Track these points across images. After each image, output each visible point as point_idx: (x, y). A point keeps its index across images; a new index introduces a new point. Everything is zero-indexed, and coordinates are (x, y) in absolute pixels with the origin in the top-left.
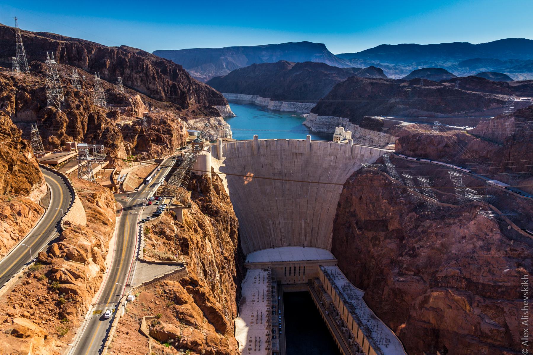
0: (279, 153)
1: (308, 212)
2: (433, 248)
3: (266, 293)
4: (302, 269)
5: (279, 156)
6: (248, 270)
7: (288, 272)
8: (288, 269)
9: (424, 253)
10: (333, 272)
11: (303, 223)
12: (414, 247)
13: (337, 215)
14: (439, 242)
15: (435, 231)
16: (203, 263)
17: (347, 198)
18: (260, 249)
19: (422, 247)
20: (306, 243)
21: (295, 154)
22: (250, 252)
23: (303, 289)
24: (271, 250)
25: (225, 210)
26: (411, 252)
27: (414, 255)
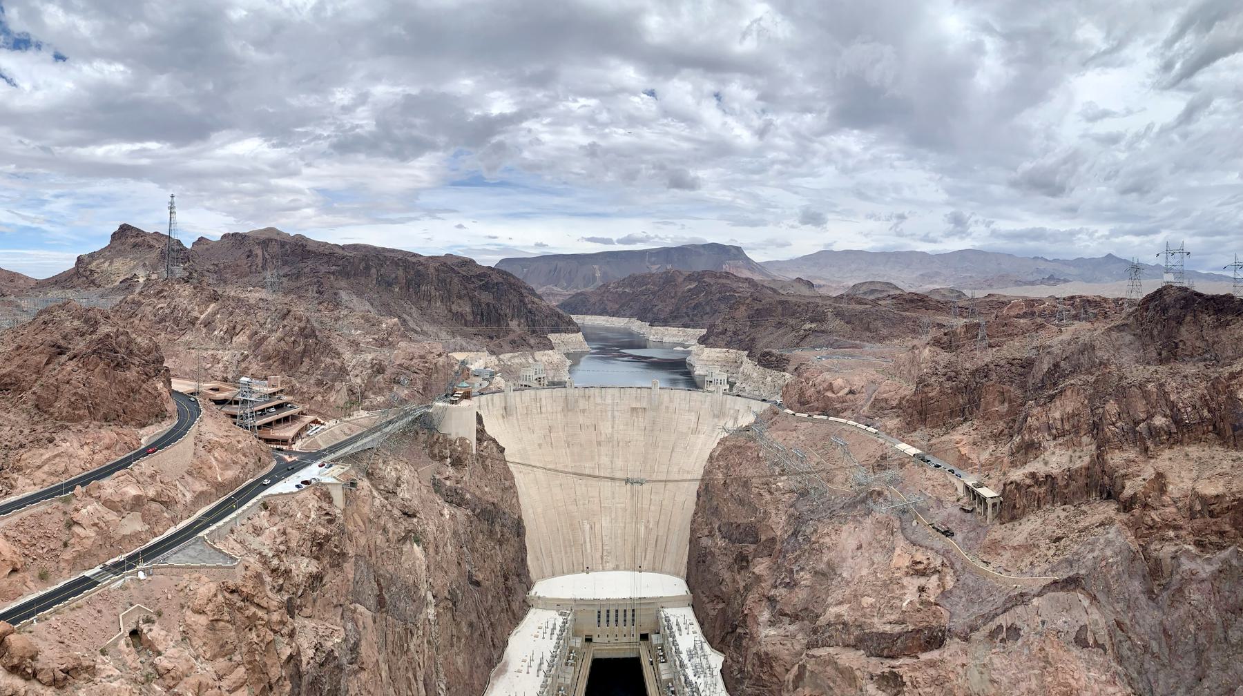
0: (609, 408)
1: (652, 508)
2: (816, 573)
3: (548, 657)
4: (629, 614)
5: (610, 414)
6: (532, 611)
7: (604, 618)
8: (603, 614)
9: (805, 578)
10: (681, 621)
11: (643, 529)
12: (792, 571)
13: (696, 514)
14: (825, 559)
15: (821, 541)
16: (379, 585)
17: (707, 485)
18: (563, 573)
19: (802, 569)
20: (645, 565)
21: (634, 410)
22: (543, 577)
23: (632, 656)
24: (583, 576)
25: (491, 500)
26: (788, 580)
27: (792, 585)
